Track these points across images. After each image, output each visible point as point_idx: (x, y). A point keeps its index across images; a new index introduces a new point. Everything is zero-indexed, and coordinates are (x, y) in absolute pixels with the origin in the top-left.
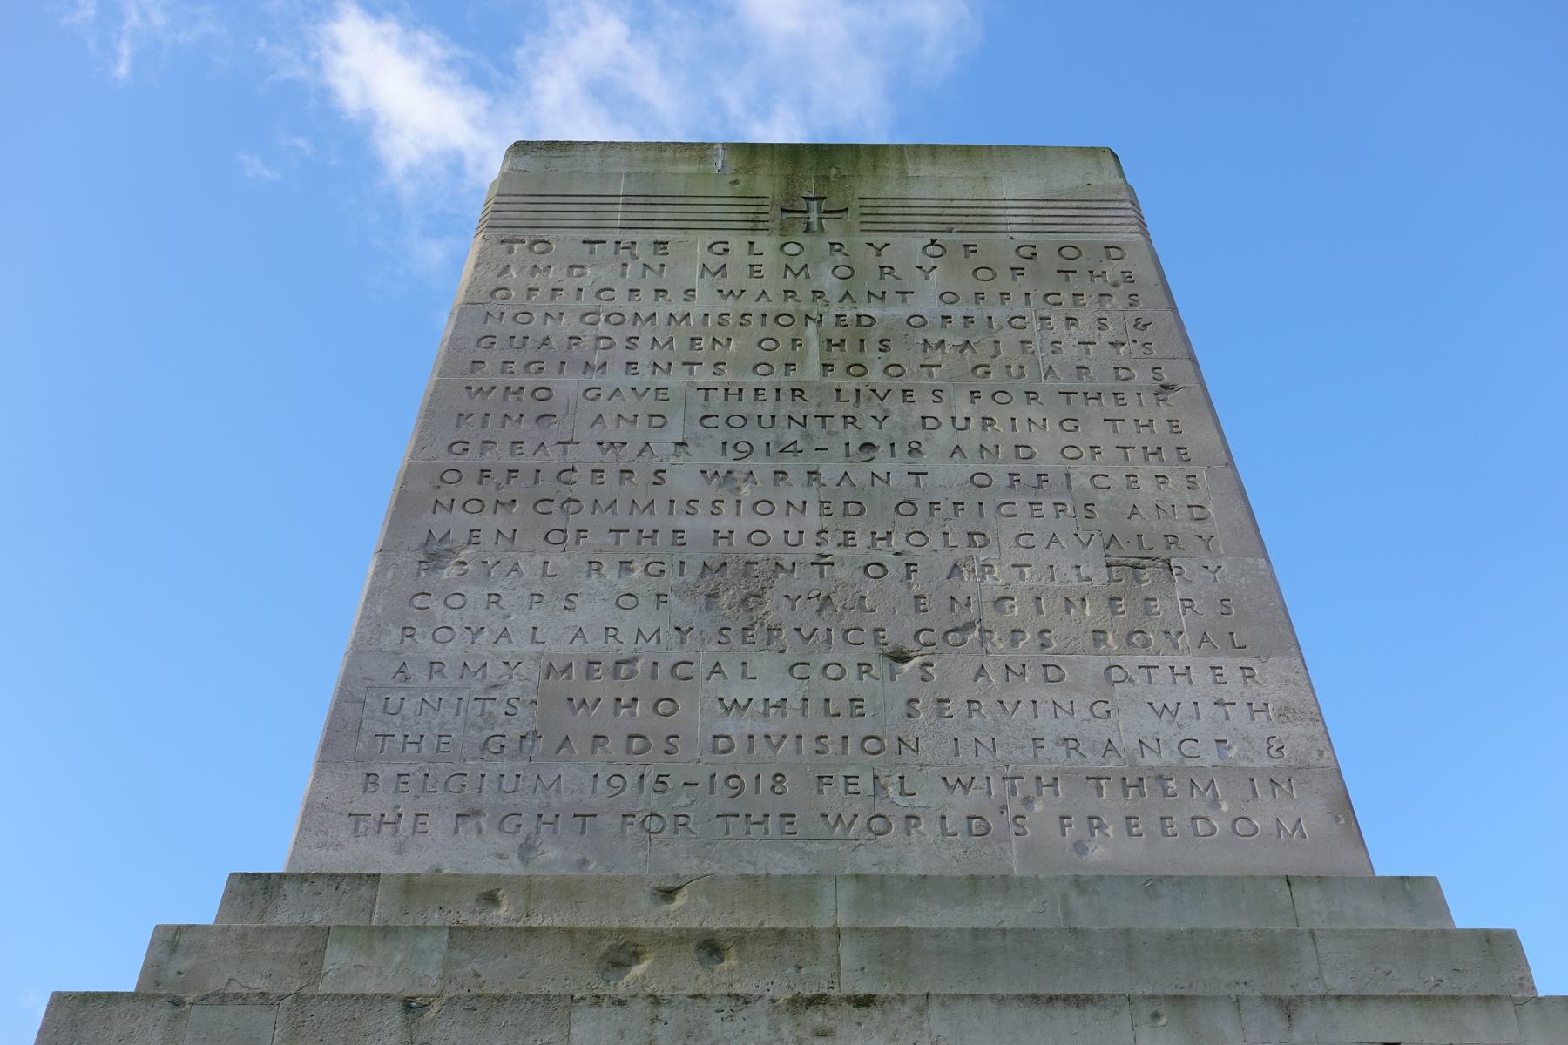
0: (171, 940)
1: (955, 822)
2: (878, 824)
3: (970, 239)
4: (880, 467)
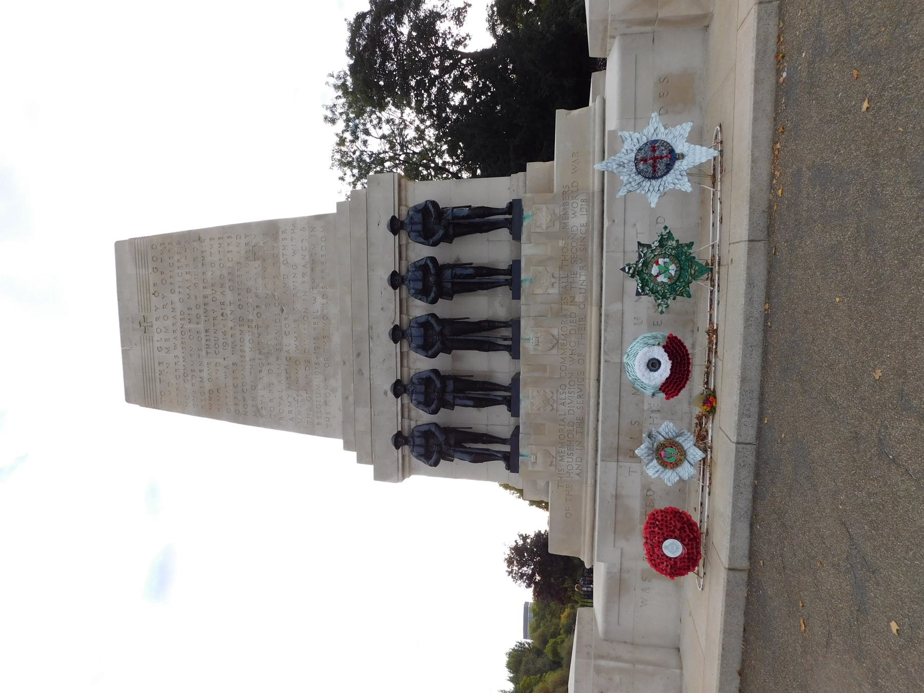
0: (360, 460)
1: (324, 301)
2: (325, 317)
3: (151, 284)
4: (229, 312)
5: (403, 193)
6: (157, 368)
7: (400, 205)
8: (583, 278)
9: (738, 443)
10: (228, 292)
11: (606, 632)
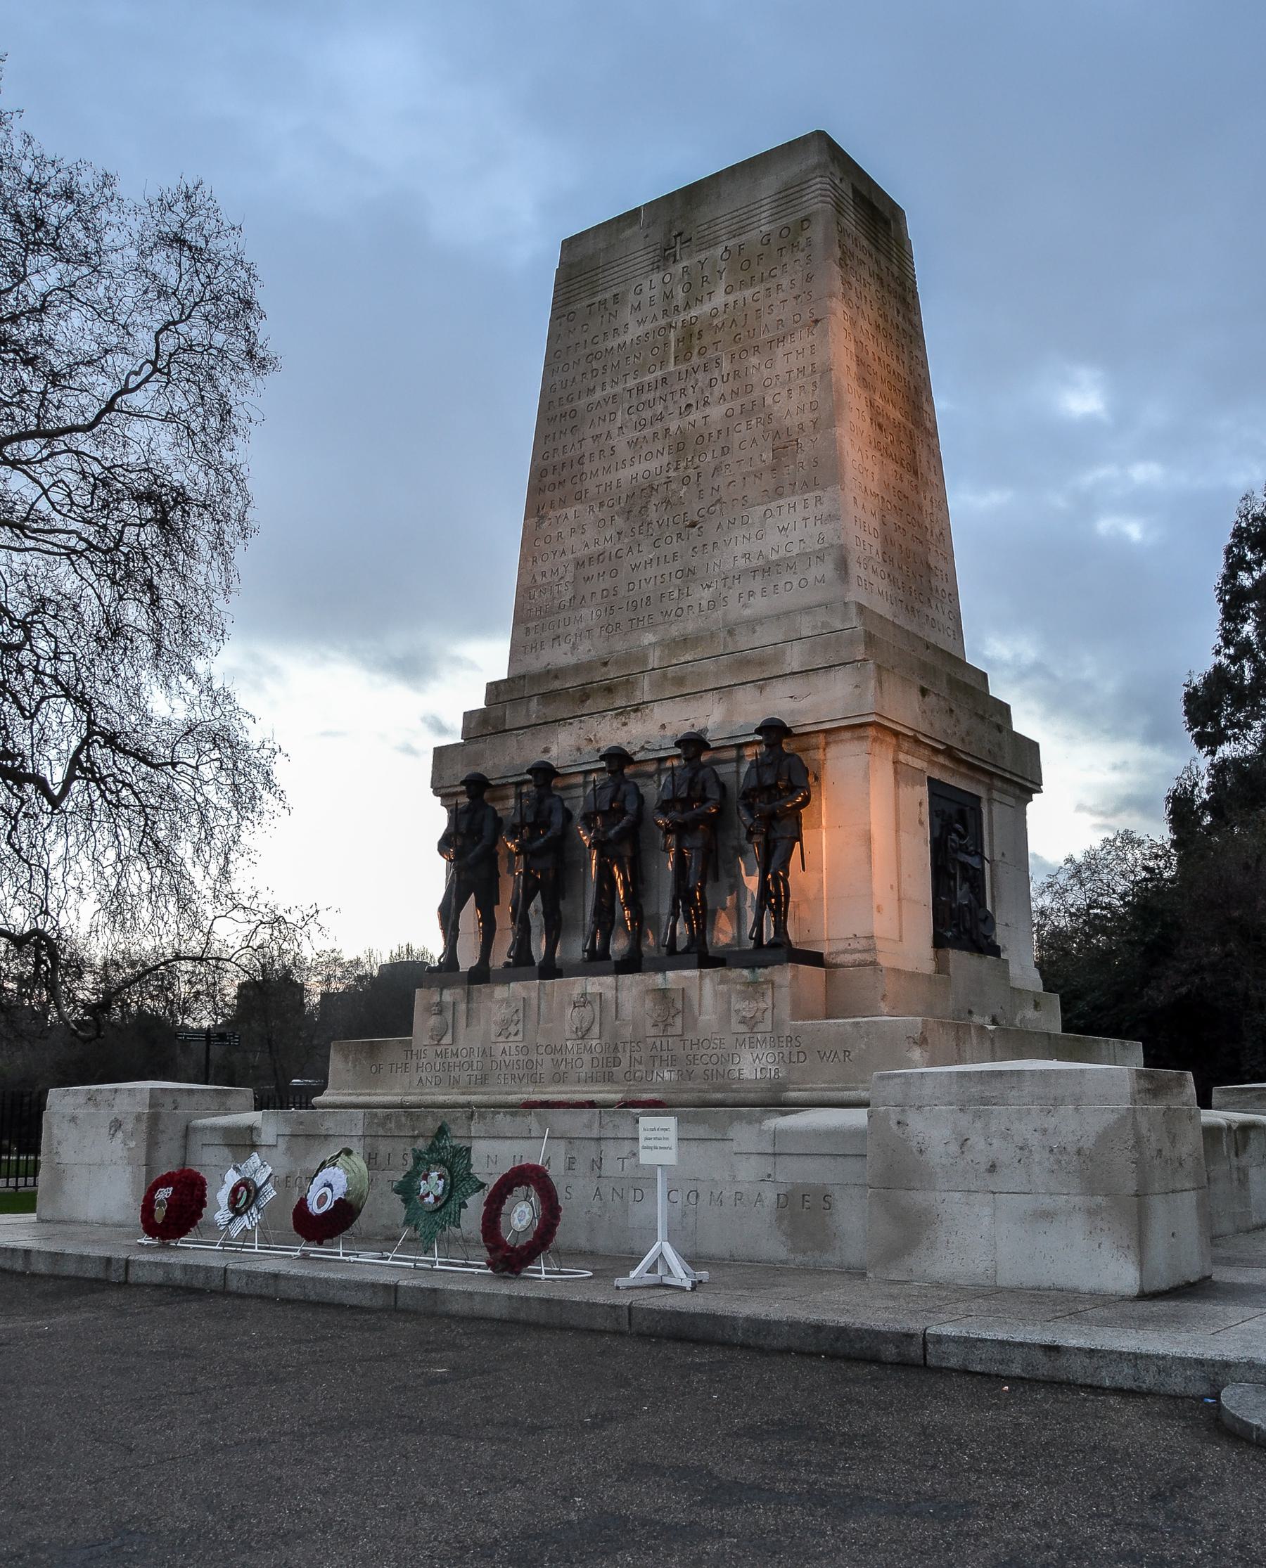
5: (847, 735)
6: (608, 295)
7: (826, 731)
8: (667, 1075)
9: (225, 1270)
10: (723, 408)
11: (195, 1129)
